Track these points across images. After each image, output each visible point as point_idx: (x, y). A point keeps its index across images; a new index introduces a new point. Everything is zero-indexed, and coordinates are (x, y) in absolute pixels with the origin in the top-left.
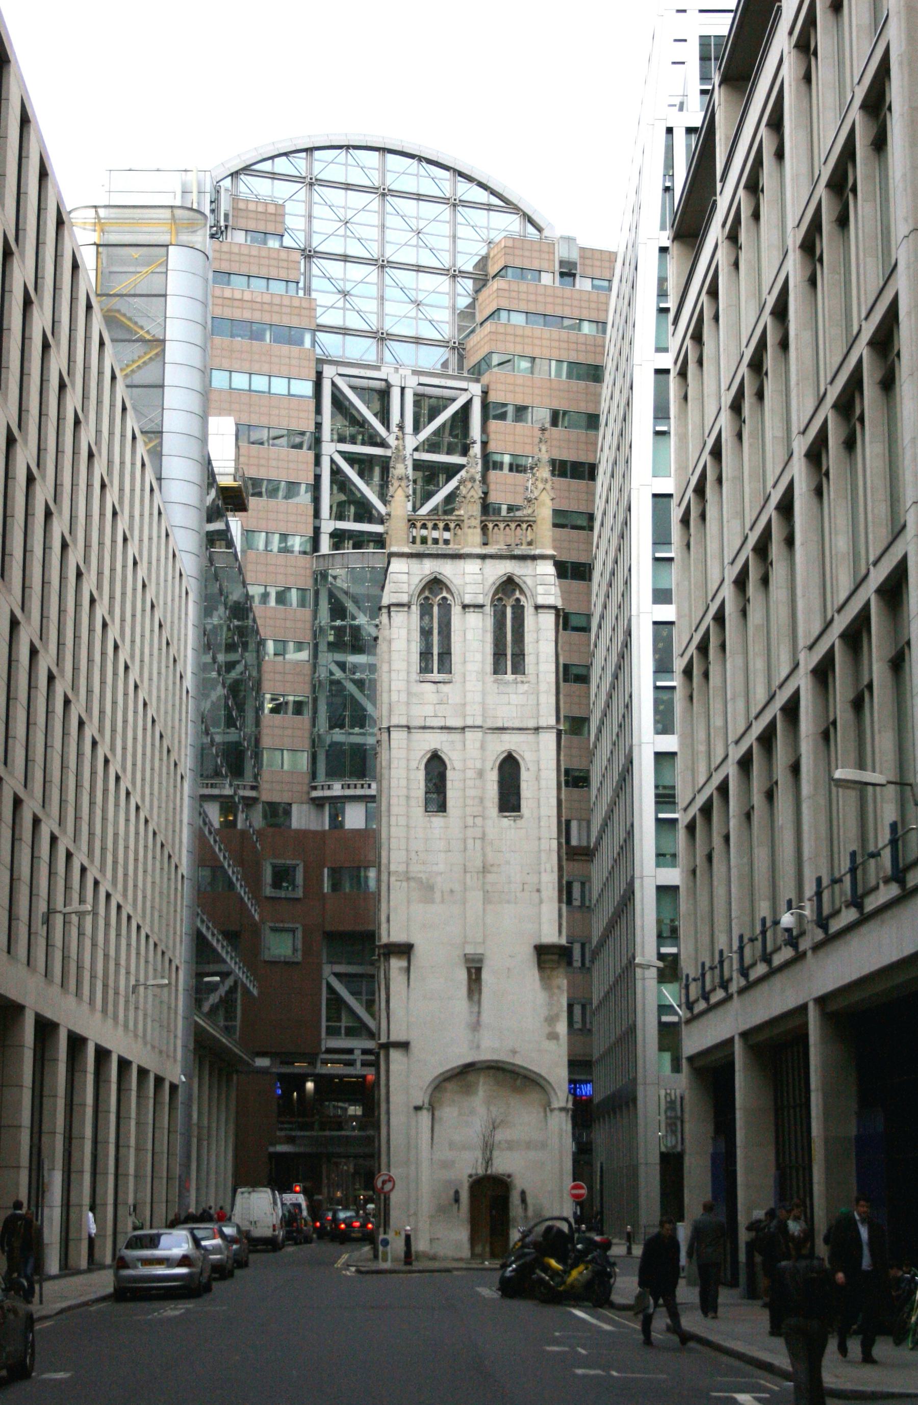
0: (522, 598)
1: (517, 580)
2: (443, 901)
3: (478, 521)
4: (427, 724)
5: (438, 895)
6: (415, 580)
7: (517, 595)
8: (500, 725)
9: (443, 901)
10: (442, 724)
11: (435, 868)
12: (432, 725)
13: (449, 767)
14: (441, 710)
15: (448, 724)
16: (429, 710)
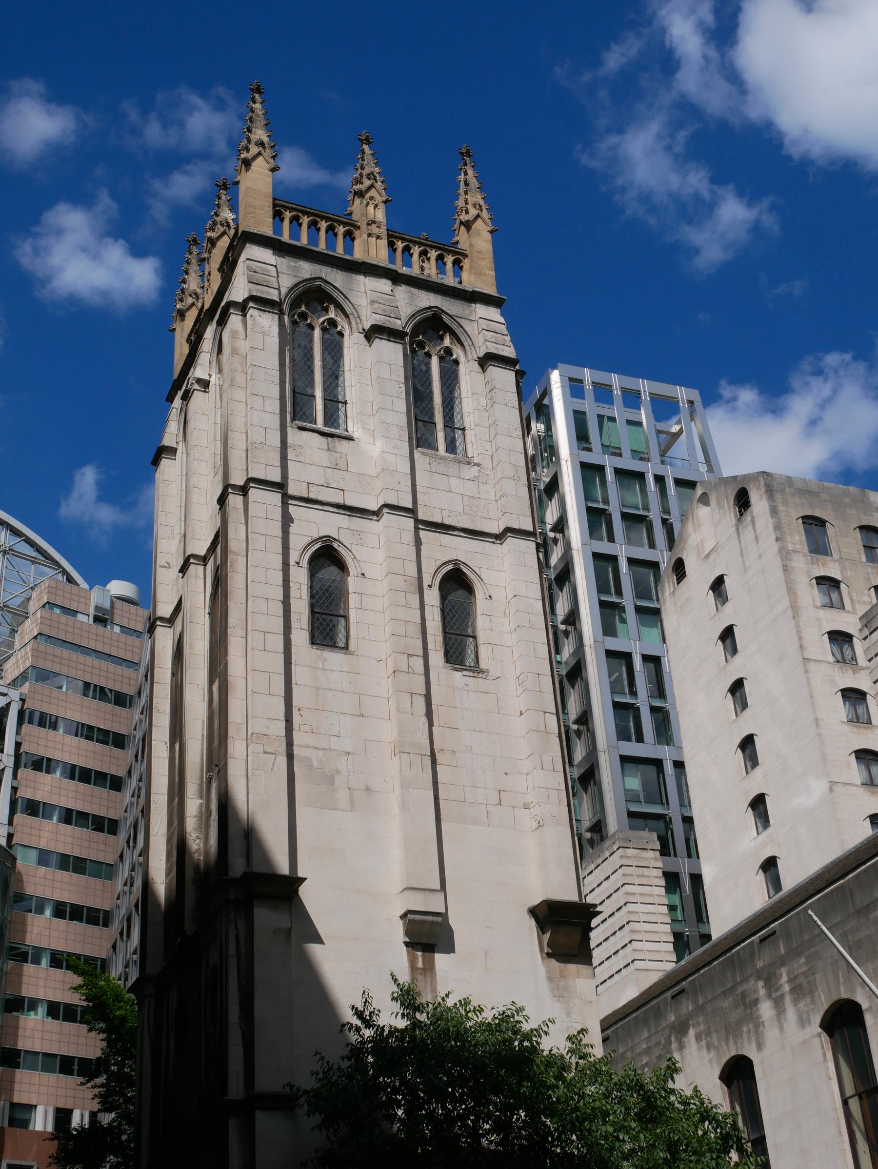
0: (457, 352)
1: (445, 318)
2: (352, 807)
3: (383, 231)
4: (312, 496)
5: (342, 795)
6: (286, 283)
7: (447, 342)
8: (437, 519)
9: (352, 807)
10: (338, 499)
11: (334, 743)
12: (320, 498)
13: (352, 570)
14: (336, 478)
15: (349, 502)
16: (315, 475)
